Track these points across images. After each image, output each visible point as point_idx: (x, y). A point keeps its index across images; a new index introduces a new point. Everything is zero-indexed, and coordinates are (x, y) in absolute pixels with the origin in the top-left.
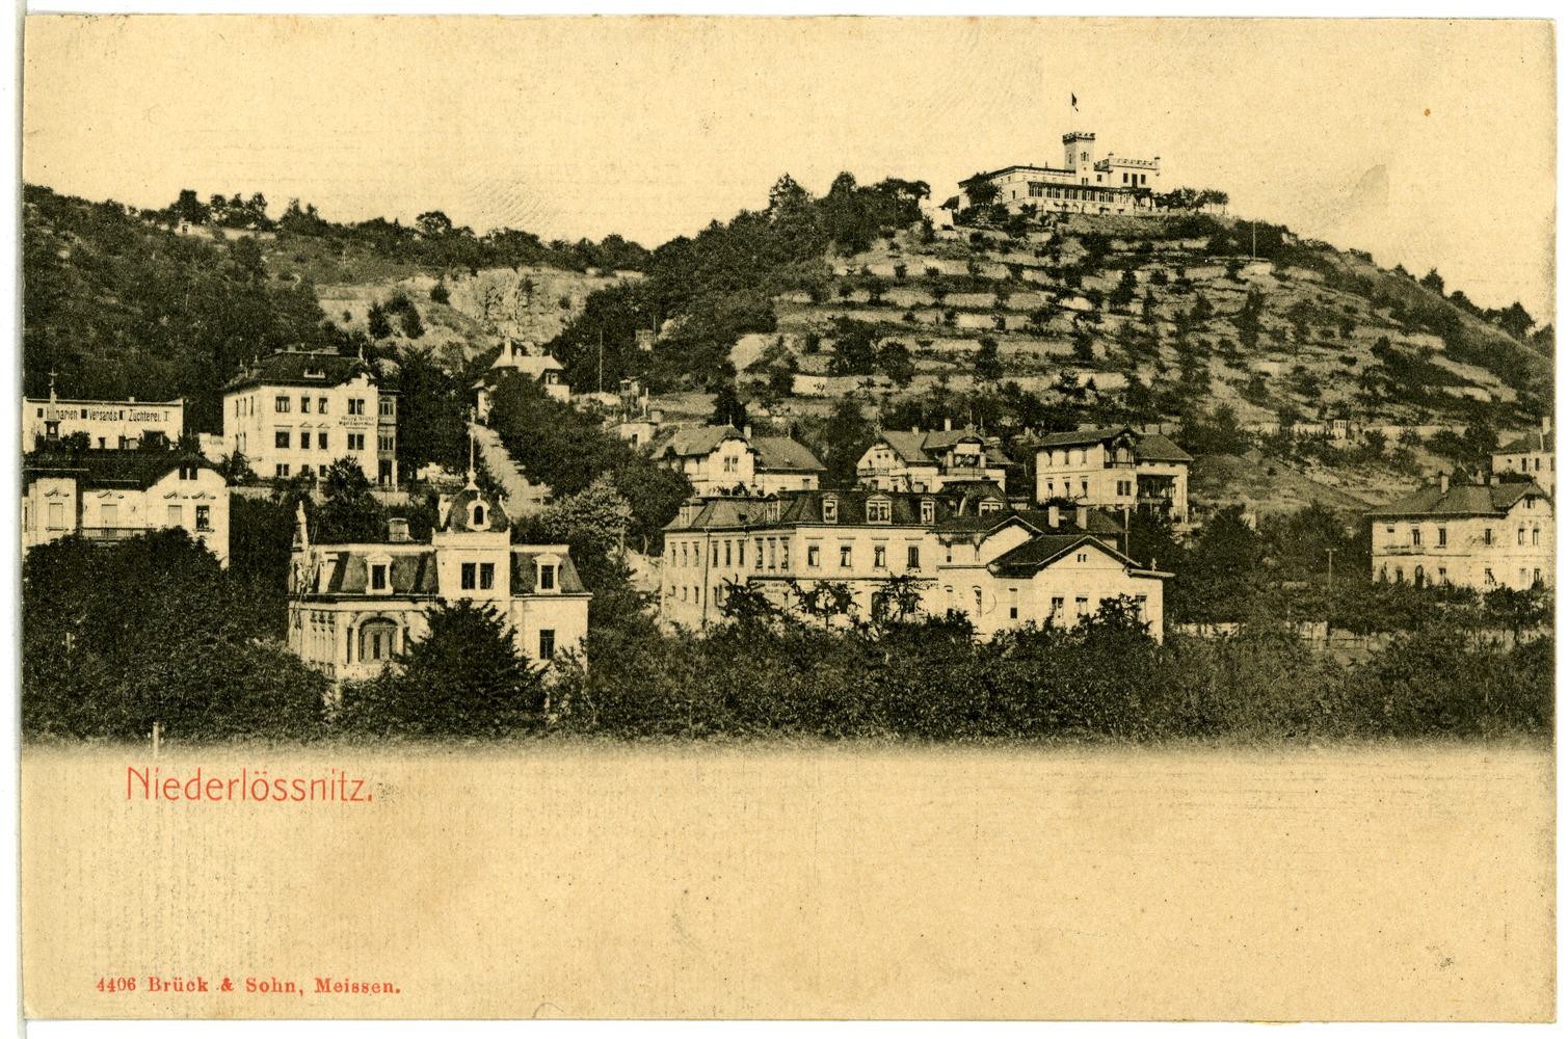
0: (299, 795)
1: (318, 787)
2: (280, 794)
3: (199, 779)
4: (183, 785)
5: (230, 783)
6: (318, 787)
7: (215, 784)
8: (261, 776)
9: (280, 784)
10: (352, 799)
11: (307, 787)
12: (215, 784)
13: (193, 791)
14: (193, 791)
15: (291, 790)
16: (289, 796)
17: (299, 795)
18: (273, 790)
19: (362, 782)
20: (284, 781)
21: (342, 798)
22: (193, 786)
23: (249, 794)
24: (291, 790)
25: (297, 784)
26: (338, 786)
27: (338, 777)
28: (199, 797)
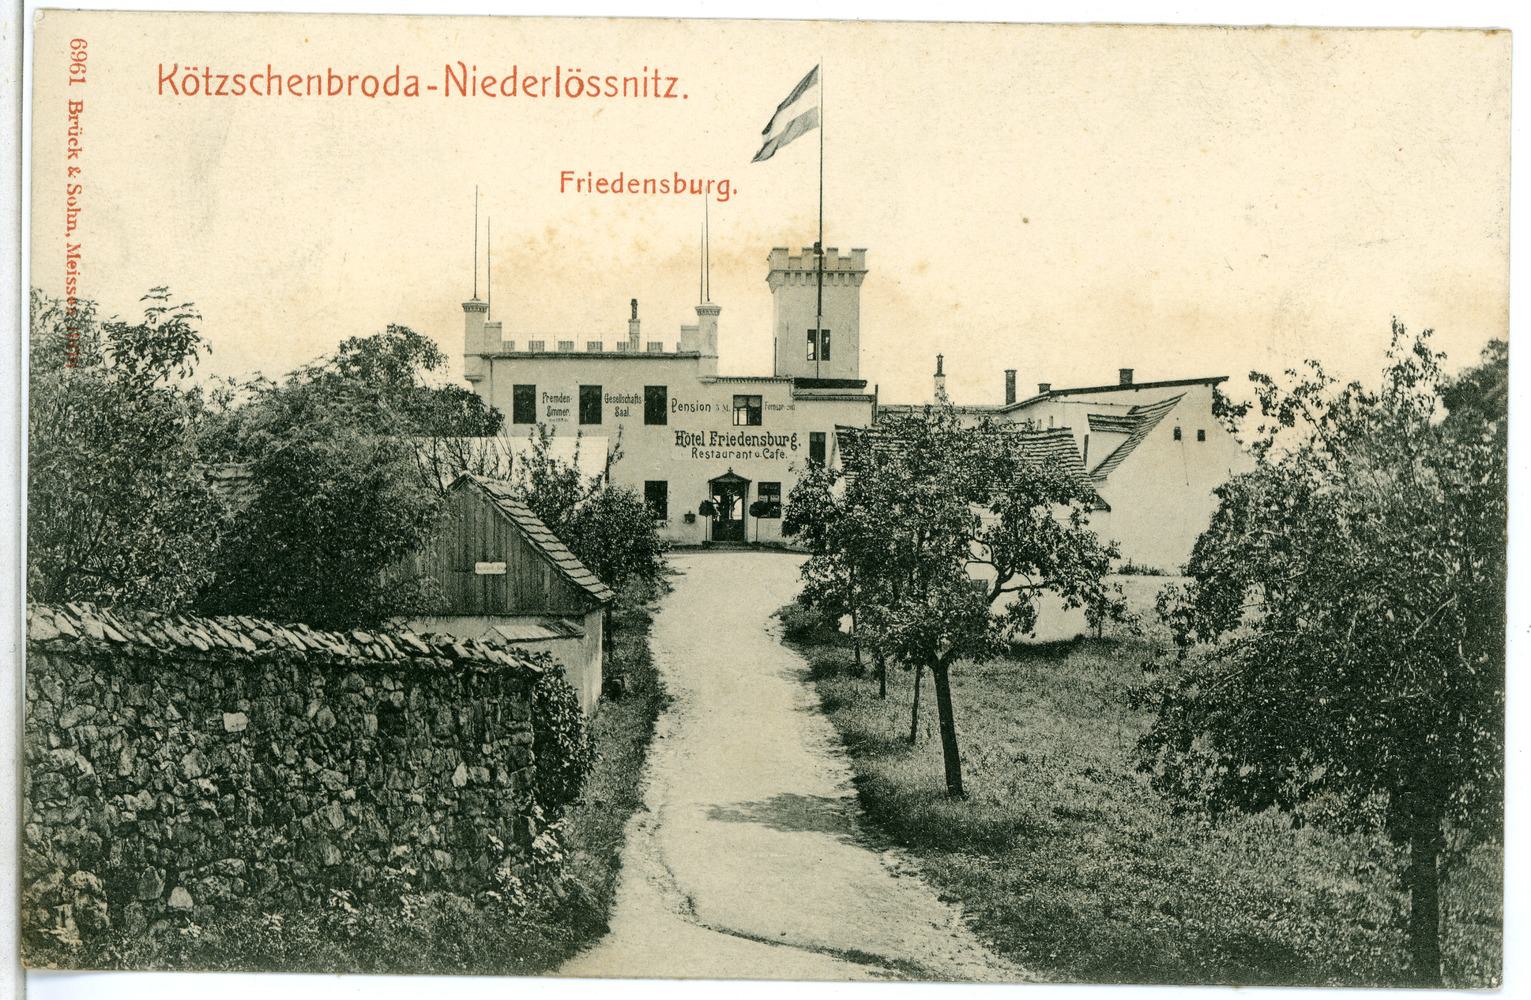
0: (611, 91)
1: (631, 84)
2: (593, 91)
3: (515, 77)
4: (499, 82)
5: (545, 80)
6: (631, 84)
7: (529, 82)
8: (575, 74)
9: (594, 81)
10: (667, 95)
11: (619, 84)
12: (529, 82)
13: (508, 89)
14: (508, 89)
15: (604, 87)
16: (602, 93)
17: (611, 91)
18: (587, 87)
19: (675, 80)
20: (598, 79)
21: (657, 95)
22: (510, 82)
23: (562, 89)
24: (602, 84)
25: (611, 81)
26: (651, 84)
27: (650, 74)
28: (514, 93)
